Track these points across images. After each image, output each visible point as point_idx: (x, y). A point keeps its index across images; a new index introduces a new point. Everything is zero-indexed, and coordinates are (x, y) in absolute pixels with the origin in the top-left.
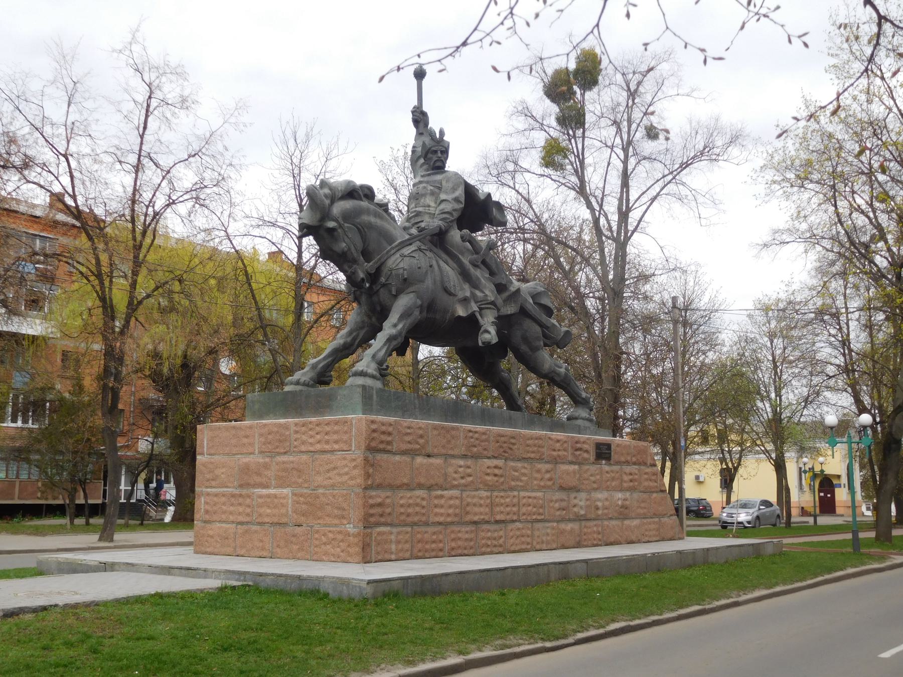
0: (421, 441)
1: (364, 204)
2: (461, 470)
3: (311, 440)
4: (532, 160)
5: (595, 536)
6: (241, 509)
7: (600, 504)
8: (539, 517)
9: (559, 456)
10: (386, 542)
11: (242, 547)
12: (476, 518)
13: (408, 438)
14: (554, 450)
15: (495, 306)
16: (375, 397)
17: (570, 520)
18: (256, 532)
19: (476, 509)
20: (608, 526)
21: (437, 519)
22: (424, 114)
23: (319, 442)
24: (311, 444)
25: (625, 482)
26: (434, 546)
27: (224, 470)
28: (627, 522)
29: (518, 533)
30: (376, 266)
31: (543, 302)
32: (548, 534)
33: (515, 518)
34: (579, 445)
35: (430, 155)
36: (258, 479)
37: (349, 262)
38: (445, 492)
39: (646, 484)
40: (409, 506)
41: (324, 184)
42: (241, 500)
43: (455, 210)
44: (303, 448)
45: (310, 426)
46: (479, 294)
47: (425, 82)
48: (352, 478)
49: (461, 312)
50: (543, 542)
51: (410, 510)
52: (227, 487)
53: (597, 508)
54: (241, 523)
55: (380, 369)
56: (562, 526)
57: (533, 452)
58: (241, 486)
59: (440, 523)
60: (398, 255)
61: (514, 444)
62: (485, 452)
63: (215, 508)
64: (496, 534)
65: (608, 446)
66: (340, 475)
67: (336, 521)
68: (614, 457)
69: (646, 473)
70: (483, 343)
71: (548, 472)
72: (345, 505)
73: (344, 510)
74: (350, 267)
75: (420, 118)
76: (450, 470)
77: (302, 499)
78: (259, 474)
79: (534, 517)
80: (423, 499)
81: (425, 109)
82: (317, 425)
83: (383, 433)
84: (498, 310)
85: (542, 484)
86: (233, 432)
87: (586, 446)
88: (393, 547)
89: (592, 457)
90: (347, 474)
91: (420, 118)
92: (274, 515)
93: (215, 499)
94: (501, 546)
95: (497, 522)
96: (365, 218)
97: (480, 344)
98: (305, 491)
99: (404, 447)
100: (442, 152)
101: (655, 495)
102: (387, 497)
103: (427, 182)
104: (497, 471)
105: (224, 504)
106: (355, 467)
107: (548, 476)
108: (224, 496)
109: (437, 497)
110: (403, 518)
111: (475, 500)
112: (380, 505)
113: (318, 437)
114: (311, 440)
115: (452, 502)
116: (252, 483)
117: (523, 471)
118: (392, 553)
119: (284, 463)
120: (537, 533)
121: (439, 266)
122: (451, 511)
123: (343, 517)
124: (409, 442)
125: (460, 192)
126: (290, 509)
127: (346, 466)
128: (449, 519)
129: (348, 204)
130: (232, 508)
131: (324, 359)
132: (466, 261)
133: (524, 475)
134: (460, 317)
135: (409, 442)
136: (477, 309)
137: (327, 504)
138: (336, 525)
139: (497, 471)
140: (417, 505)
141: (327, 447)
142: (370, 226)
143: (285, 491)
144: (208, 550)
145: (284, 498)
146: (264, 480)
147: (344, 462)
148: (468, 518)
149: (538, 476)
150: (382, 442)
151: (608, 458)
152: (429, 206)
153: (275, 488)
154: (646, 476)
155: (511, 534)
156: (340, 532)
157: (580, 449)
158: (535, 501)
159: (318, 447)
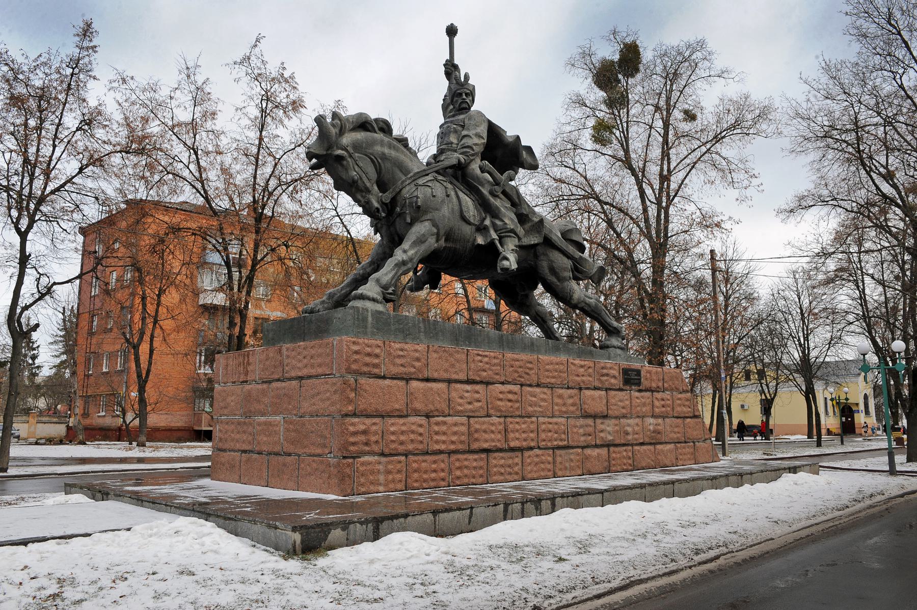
0: (417, 364)
1: (379, 136)
2: (466, 395)
3: (299, 365)
4: (586, 139)
5: (625, 461)
7: (629, 429)
8: (561, 443)
9: (583, 382)
10: (372, 472)
12: (486, 446)
13: (398, 361)
14: (578, 376)
15: (515, 234)
16: (370, 319)
17: (596, 446)
19: (486, 436)
20: (639, 451)
21: (437, 447)
22: (456, 67)
24: (299, 368)
25: (657, 407)
26: (433, 475)
27: (233, 398)
28: (659, 447)
29: (536, 460)
30: (391, 196)
31: (574, 238)
32: (572, 460)
33: (532, 444)
34: (605, 371)
35: (455, 99)
37: (362, 191)
38: (448, 419)
39: (679, 409)
40: (403, 433)
41: (335, 115)
43: (476, 144)
46: (498, 223)
47: (456, 39)
49: (480, 241)
50: (566, 468)
51: (402, 438)
53: (627, 434)
54: (245, 451)
55: (383, 293)
56: (588, 451)
57: (554, 377)
59: (441, 452)
60: (412, 185)
61: (531, 369)
62: (497, 377)
64: (510, 462)
66: (323, 400)
68: (645, 383)
69: (679, 399)
70: (502, 269)
71: (571, 397)
72: (326, 433)
74: (364, 197)
75: (451, 69)
76: (454, 394)
77: (291, 426)
78: (259, 401)
79: (555, 443)
80: (421, 426)
81: (456, 62)
83: (369, 355)
84: (519, 239)
85: (564, 409)
87: (612, 372)
88: (382, 478)
89: (617, 382)
90: (328, 399)
91: (451, 69)
94: (517, 473)
95: (512, 450)
96: (378, 149)
99: (395, 370)
100: (467, 95)
101: (689, 420)
102: (374, 424)
103: (451, 122)
104: (510, 396)
106: (335, 392)
107: (570, 401)
108: (232, 423)
109: (437, 424)
110: (393, 446)
111: (484, 427)
112: (364, 432)
113: (305, 361)
115: (456, 429)
117: (542, 396)
118: (380, 484)
119: (277, 389)
120: (559, 459)
121: (458, 197)
122: (454, 438)
124: (402, 365)
125: (483, 130)
128: (452, 447)
129: (360, 136)
130: (238, 436)
131: (342, 289)
132: (485, 191)
133: (544, 400)
135: (402, 365)
136: (496, 237)
139: (510, 396)
140: (413, 432)
142: (384, 157)
147: (327, 386)
148: (475, 446)
149: (560, 401)
150: (367, 365)
151: (639, 384)
152: (452, 143)
154: (679, 402)
155: (529, 461)
157: (607, 375)
158: (556, 427)
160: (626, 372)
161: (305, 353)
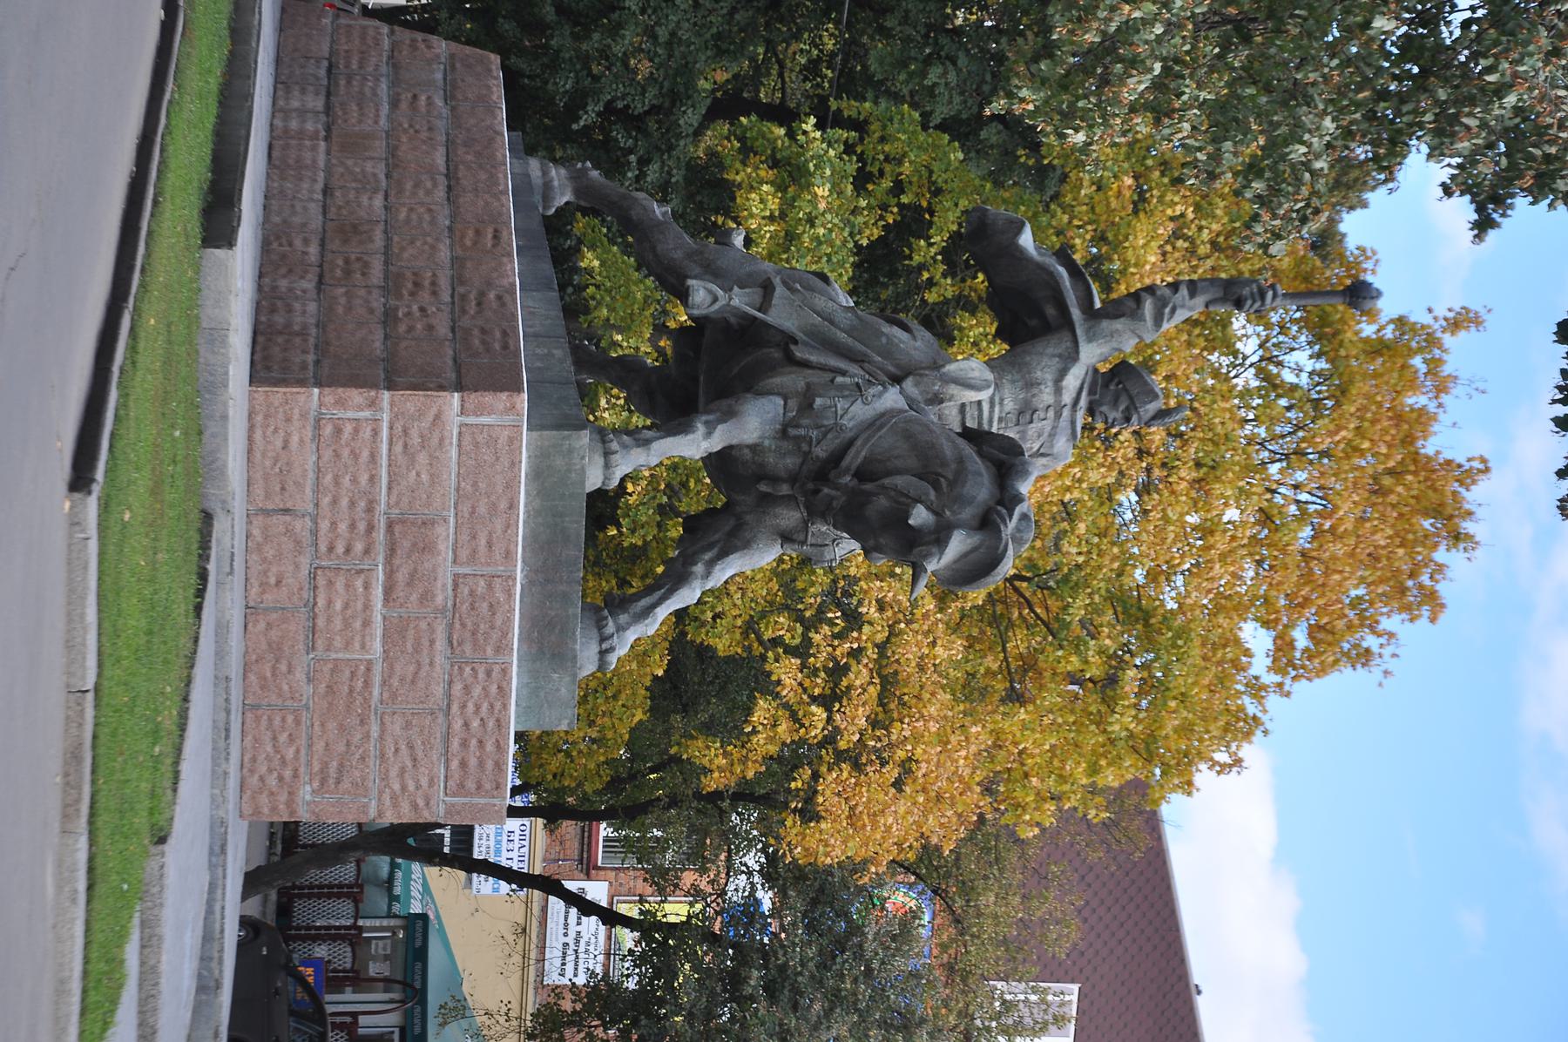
3: (471, 707)
6: (343, 527)
11: (265, 529)
18: (297, 566)
23: (466, 725)
36: (401, 576)
42: (362, 526)
44: (457, 688)
45: (498, 706)
48: (394, 797)
52: (389, 489)
54: (315, 533)
58: (390, 526)
63: (346, 453)
66: (403, 771)
67: (316, 767)
72: (346, 785)
73: (338, 782)
77: (360, 684)
82: (498, 720)
86: (503, 505)
90: (404, 788)
92: (329, 620)
93: (365, 454)
98: (376, 692)
105: (354, 481)
113: (475, 724)
114: (471, 707)
116: (397, 562)
123: (323, 782)
126: (340, 655)
127: (418, 787)
130: (345, 502)
137: (348, 744)
138: (309, 764)
141: (455, 744)
143: (377, 646)
144: (258, 435)
145: (363, 646)
146: (399, 593)
147: (424, 782)
153: (385, 618)
156: (296, 776)
159: (457, 725)
161: (491, 724)
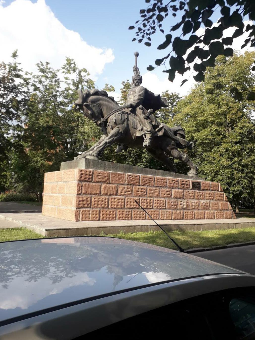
7: (193, 204)
60: (113, 115)
61: (152, 181)
65: (199, 183)
68: (202, 188)
81: (138, 66)
96: (101, 102)
97: (144, 146)
134: (137, 137)
160: (193, 183)
